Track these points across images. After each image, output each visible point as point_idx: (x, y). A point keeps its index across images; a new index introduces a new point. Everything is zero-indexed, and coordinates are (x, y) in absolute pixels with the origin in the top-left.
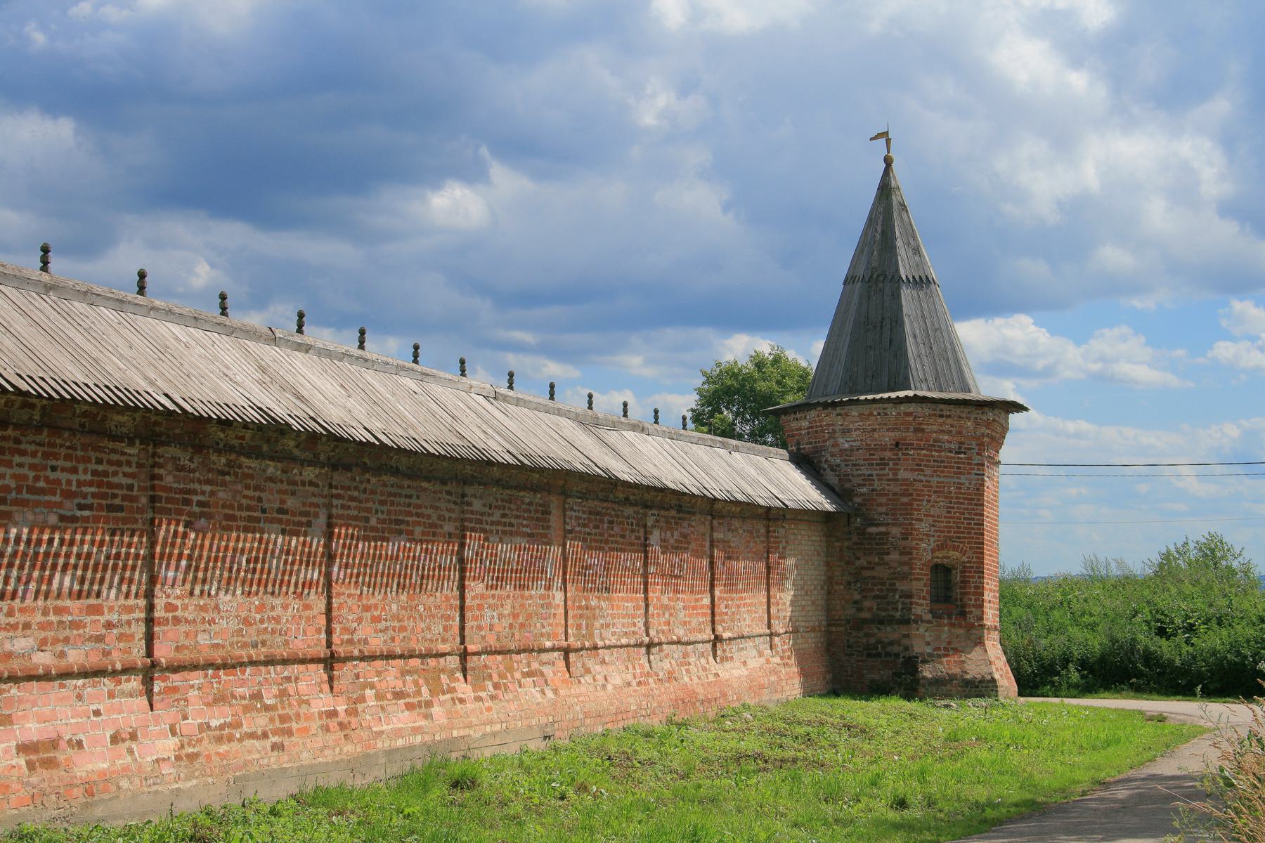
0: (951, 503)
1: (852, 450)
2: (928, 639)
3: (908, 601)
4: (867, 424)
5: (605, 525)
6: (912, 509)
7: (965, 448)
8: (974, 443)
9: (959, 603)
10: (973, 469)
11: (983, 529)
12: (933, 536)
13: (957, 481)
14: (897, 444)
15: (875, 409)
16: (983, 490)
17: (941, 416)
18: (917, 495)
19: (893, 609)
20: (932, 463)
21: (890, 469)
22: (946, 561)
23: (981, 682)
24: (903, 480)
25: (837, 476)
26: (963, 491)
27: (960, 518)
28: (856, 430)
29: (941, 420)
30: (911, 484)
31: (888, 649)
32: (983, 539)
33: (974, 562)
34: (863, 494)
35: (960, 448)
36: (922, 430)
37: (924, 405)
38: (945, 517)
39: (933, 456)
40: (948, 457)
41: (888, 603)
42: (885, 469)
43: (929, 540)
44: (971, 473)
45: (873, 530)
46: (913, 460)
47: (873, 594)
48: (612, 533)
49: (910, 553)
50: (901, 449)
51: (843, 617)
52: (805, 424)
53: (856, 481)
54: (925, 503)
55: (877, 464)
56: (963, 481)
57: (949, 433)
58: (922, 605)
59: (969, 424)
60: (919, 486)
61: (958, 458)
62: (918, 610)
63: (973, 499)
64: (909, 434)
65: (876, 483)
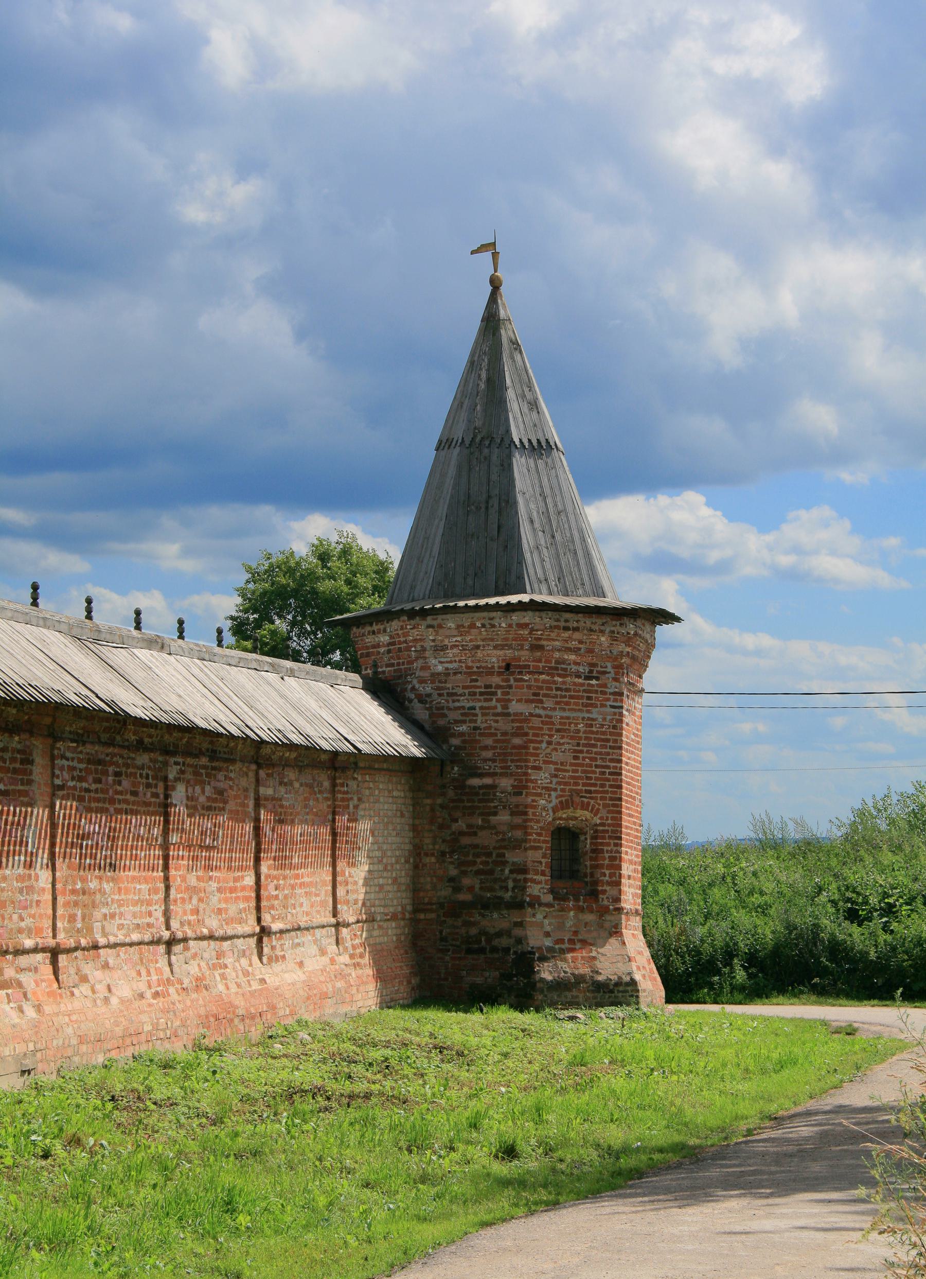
0: (578, 745)
1: (448, 675)
2: (548, 929)
3: (521, 877)
4: (468, 638)
5: (110, 779)
6: (527, 754)
7: (598, 672)
8: (609, 664)
9: (588, 879)
10: (608, 700)
11: (621, 780)
12: (555, 790)
13: (586, 715)
14: (508, 667)
15: (479, 619)
16: (622, 729)
17: (566, 629)
18: (534, 735)
19: (501, 888)
20: (554, 692)
21: (498, 700)
22: (571, 823)
23: (617, 984)
24: (516, 714)
25: (427, 709)
26: (594, 729)
27: (591, 766)
29: (566, 634)
30: (526, 720)
31: (496, 942)
32: (621, 793)
33: (609, 825)
34: (462, 734)
35: (591, 671)
36: (541, 648)
37: (544, 614)
38: (571, 764)
39: (555, 682)
40: (575, 684)
41: (495, 880)
42: (491, 700)
43: (550, 795)
44: (605, 706)
45: (475, 782)
46: (529, 687)
47: (475, 868)
48: (119, 788)
49: (526, 813)
50: (513, 673)
51: (435, 900)
52: (384, 639)
53: (453, 716)
54: (544, 745)
55: (481, 694)
56: (594, 716)
57: (576, 651)
58: (540, 883)
59: (603, 639)
60: (536, 722)
61: (589, 685)
62: (534, 890)
63: (608, 740)
65: (479, 718)
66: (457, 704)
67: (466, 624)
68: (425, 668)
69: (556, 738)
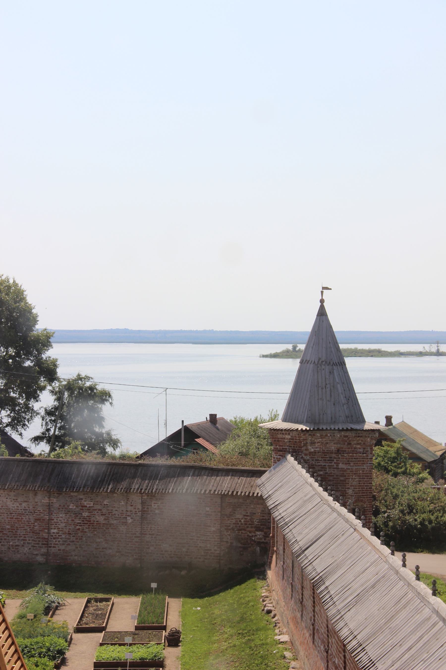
0: (360, 479)
8: (369, 448)
10: (368, 461)
12: (354, 496)
13: (362, 467)
14: (338, 450)
15: (329, 433)
17: (359, 437)
21: (335, 463)
24: (341, 468)
28: (318, 443)
29: (358, 439)
30: (345, 471)
35: (364, 451)
39: (353, 456)
40: (359, 456)
42: (332, 463)
46: (346, 459)
50: (340, 453)
54: (351, 480)
55: (328, 460)
57: (358, 444)
64: (345, 446)
65: (328, 469)
66: (319, 464)
67: (324, 435)
68: (307, 450)
69: (354, 477)
